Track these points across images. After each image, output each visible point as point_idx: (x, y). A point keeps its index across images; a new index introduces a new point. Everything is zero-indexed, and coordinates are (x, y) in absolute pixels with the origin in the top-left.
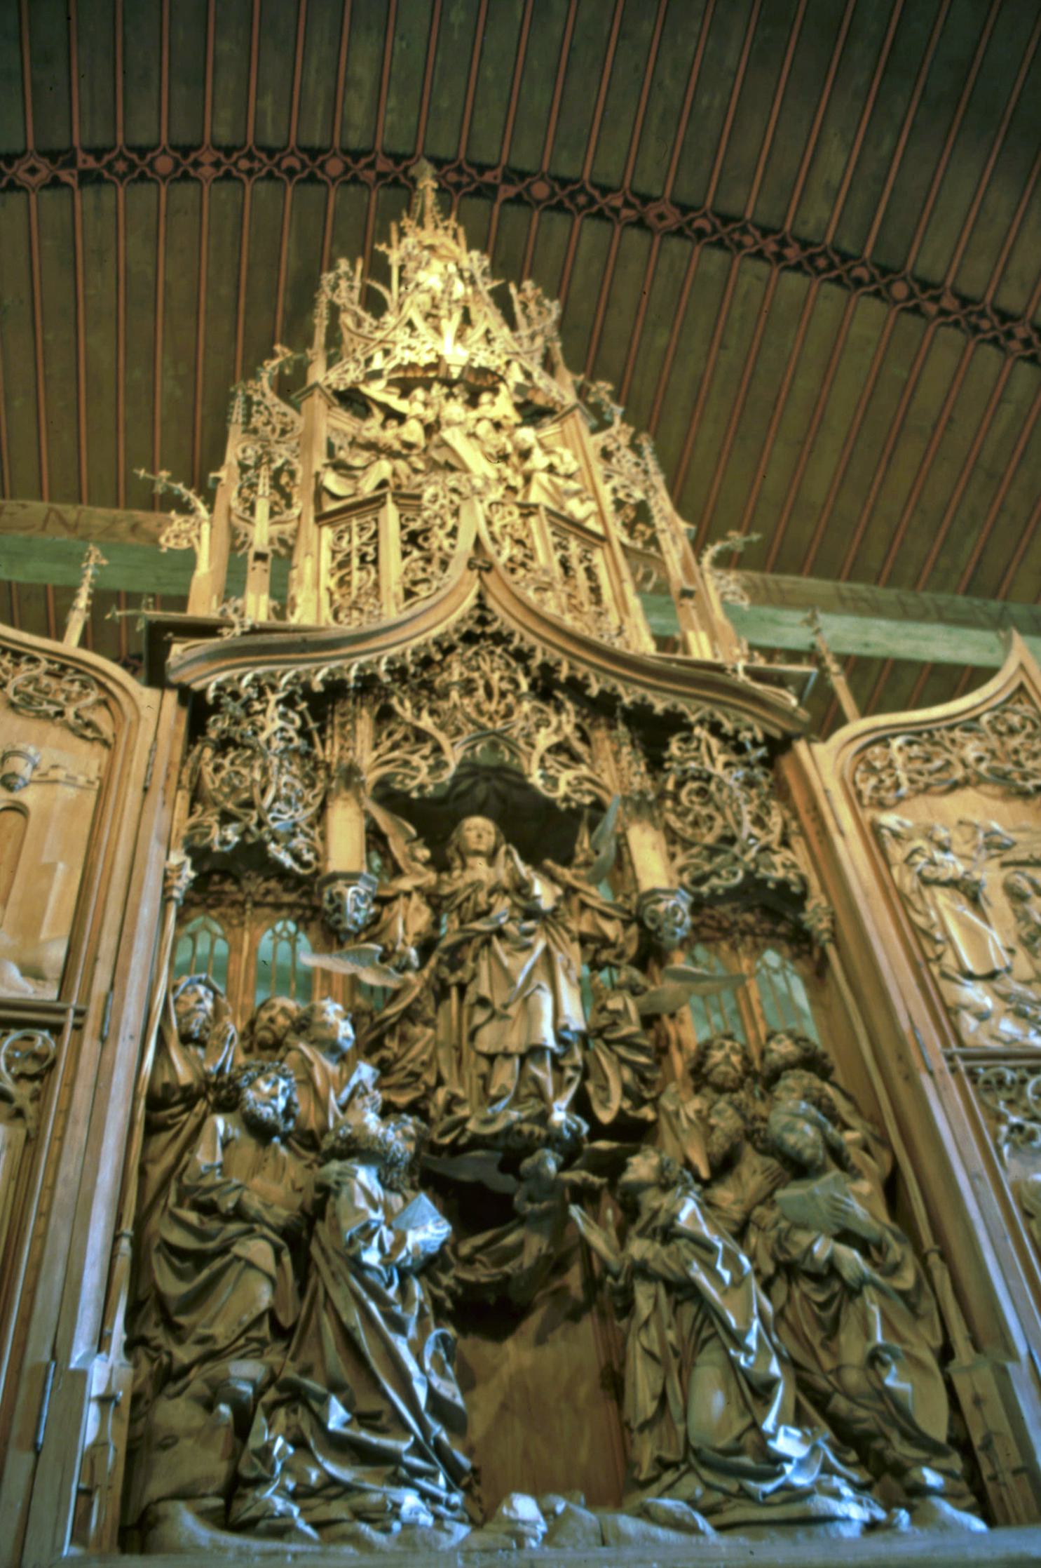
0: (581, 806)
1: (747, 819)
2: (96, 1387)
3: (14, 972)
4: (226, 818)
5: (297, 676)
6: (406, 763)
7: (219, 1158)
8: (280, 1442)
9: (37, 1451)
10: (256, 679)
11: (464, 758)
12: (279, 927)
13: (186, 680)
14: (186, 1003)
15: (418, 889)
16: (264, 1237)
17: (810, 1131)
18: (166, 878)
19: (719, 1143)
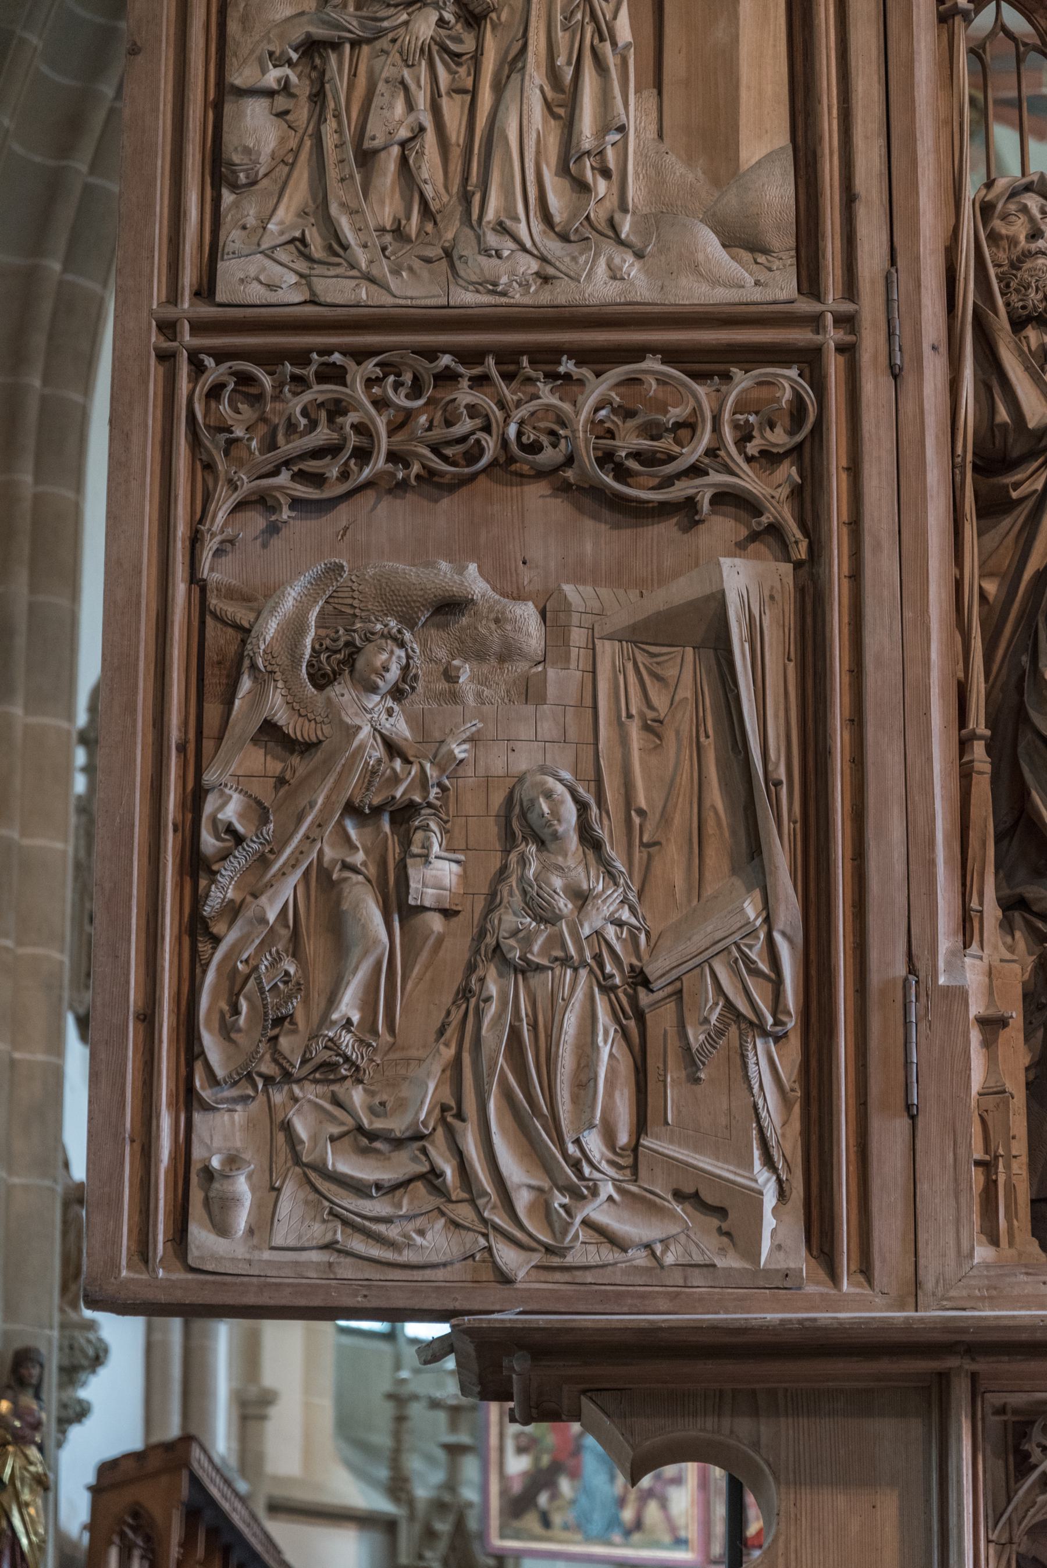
2: (976, 1008)
3: (709, 243)
14: (1013, 241)
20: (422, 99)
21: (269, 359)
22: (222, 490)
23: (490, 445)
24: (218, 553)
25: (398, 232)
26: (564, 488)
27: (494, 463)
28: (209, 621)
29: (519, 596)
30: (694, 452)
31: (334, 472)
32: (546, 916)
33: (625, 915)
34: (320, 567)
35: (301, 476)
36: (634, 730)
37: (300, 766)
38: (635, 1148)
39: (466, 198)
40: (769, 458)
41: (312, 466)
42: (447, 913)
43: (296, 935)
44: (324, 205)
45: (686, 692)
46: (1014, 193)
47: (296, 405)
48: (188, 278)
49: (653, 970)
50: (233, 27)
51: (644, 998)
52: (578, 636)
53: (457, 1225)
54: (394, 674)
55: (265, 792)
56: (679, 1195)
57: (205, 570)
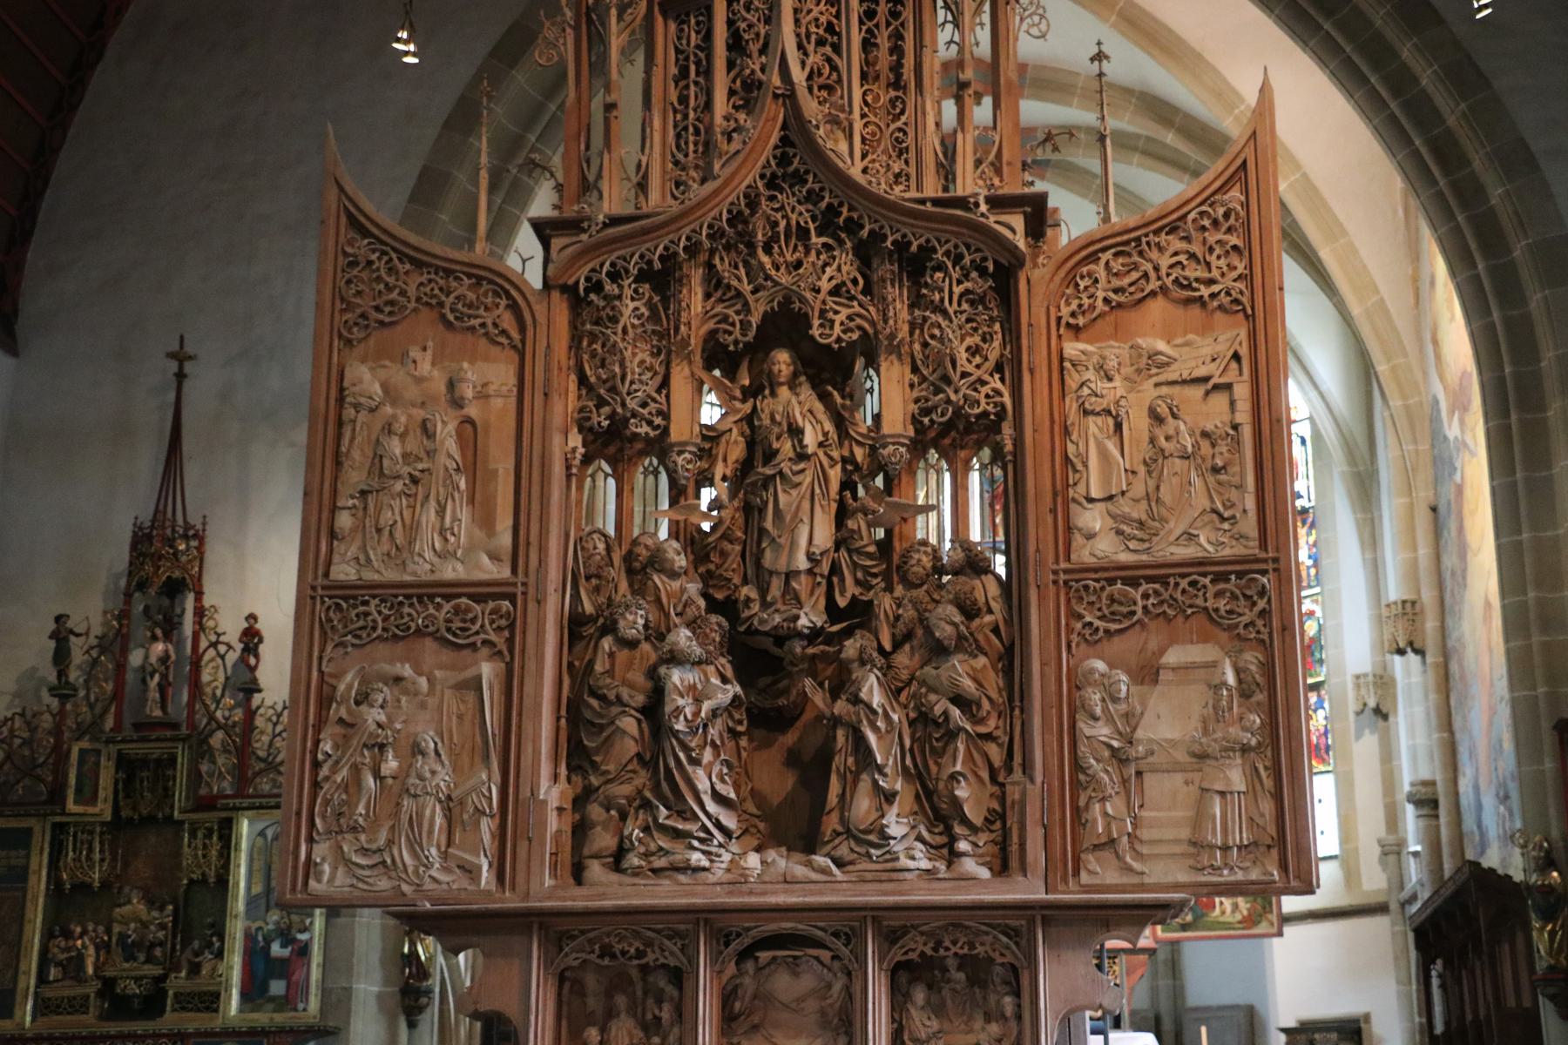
0: (852, 344)
1: (962, 355)
2: (555, 804)
3: (485, 559)
4: (601, 403)
5: (642, 257)
6: (725, 319)
7: (607, 666)
8: (637, 831)
9: (530, 840)
10: (613, 265)
11: (766, 313)
12: (647, 462)
13: (561, 282)
15: (736, 422)
16: (631, 716)
17: (949, 629)
18: (567, 459)
19: (901, 628)
20: (397, 511)
21: (345, 598)
22: (329, 642)
23: (413, 625)
24: (329, 661)
25: (388, 555)
26: (436, 639)
27: (416, 631)
28: (325, 686)
29: (420, 674)
30: (477, 627)
31: (364, 635)
32: (422, 779)
33: (447, 778)
34: (357, 668)
35: (356, 637)
36: (454, 718)
37: (351, 731)
38: (446, 852)
39: (410, 543)
40: (500, 629)
41: (359, 632)
42: (394, 778)
43: (347, 786)
44: (365, 546)
45: (470, 706)
46: (590, 533)
47: (353, 613)
48: (320, 573)
49: (453, 796)
50: (339, 485)
51: (451, 805)
52: (438, 687)
53: (390, 878)
54: (380, 701)
55: (340, 741)
56: (459, 867)
57: (324, 668)
